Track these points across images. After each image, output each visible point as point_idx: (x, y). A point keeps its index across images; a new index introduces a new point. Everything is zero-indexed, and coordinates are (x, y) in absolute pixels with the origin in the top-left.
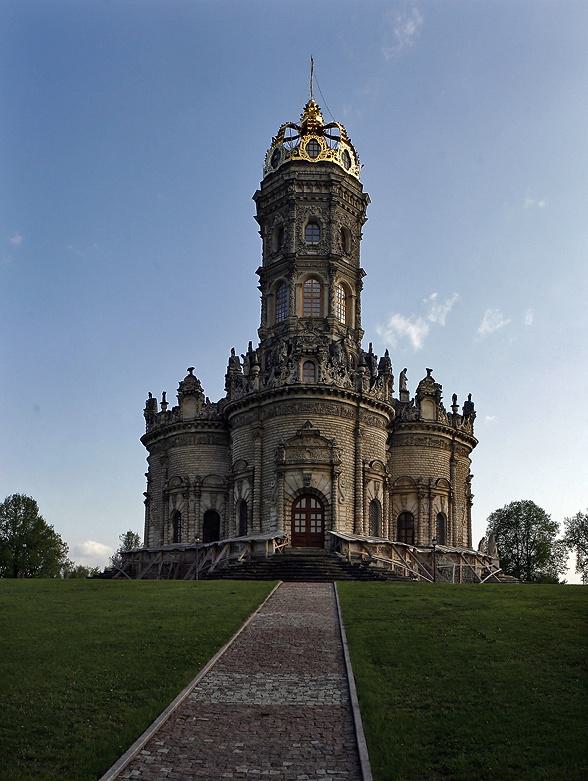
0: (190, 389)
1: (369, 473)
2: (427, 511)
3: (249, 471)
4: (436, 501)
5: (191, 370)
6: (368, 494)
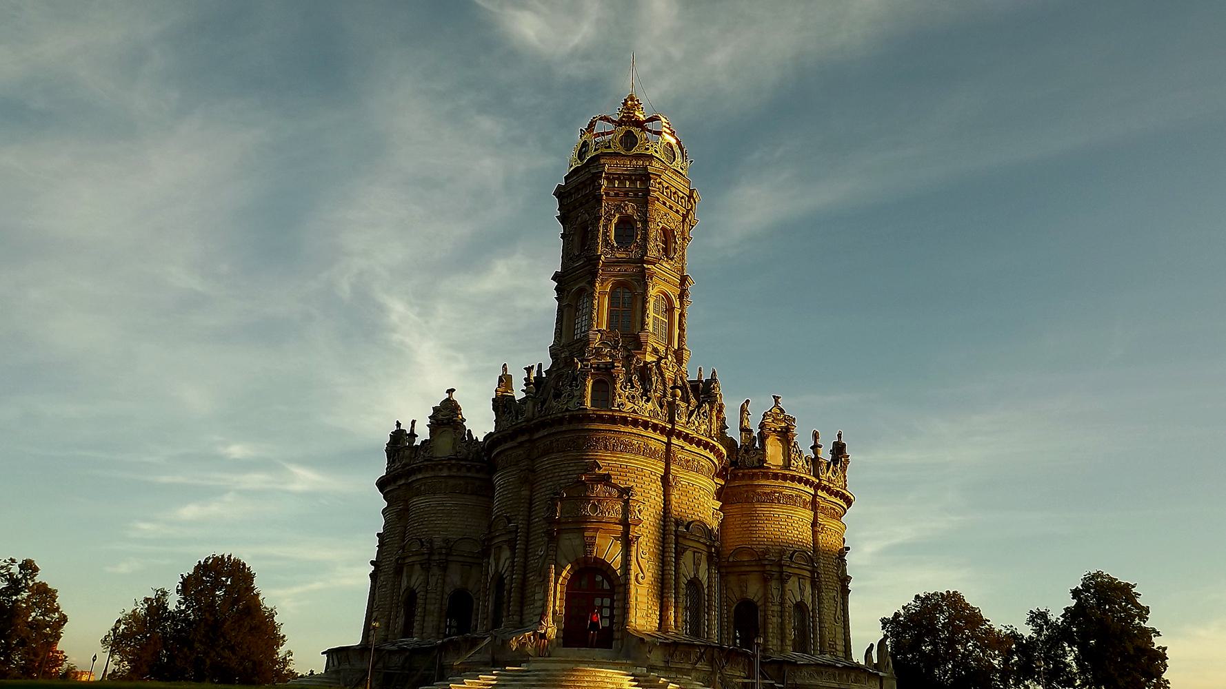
0: (447, 416)
1: (685, 538)
2: (777, 600)
3: (510, 532)
4: (792, 584)
5: (450, 391)
6: (683, 569)
